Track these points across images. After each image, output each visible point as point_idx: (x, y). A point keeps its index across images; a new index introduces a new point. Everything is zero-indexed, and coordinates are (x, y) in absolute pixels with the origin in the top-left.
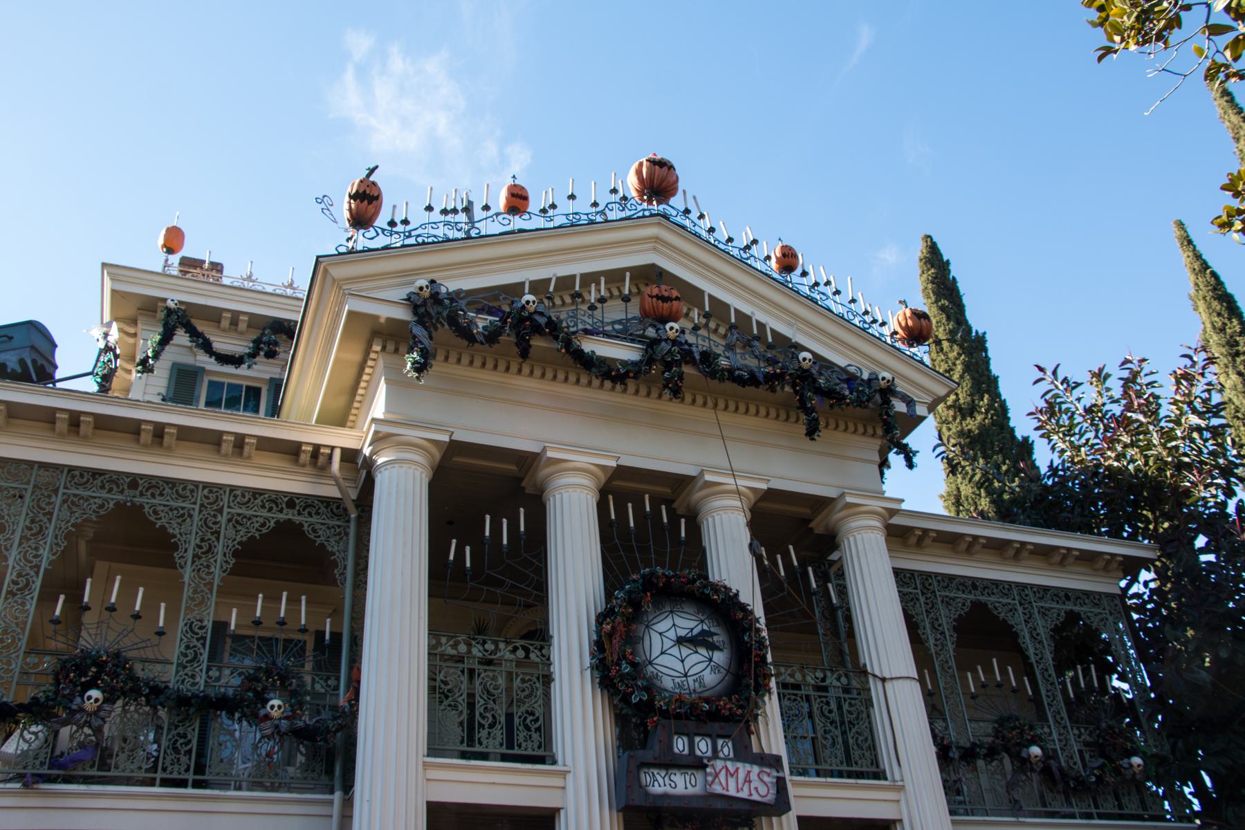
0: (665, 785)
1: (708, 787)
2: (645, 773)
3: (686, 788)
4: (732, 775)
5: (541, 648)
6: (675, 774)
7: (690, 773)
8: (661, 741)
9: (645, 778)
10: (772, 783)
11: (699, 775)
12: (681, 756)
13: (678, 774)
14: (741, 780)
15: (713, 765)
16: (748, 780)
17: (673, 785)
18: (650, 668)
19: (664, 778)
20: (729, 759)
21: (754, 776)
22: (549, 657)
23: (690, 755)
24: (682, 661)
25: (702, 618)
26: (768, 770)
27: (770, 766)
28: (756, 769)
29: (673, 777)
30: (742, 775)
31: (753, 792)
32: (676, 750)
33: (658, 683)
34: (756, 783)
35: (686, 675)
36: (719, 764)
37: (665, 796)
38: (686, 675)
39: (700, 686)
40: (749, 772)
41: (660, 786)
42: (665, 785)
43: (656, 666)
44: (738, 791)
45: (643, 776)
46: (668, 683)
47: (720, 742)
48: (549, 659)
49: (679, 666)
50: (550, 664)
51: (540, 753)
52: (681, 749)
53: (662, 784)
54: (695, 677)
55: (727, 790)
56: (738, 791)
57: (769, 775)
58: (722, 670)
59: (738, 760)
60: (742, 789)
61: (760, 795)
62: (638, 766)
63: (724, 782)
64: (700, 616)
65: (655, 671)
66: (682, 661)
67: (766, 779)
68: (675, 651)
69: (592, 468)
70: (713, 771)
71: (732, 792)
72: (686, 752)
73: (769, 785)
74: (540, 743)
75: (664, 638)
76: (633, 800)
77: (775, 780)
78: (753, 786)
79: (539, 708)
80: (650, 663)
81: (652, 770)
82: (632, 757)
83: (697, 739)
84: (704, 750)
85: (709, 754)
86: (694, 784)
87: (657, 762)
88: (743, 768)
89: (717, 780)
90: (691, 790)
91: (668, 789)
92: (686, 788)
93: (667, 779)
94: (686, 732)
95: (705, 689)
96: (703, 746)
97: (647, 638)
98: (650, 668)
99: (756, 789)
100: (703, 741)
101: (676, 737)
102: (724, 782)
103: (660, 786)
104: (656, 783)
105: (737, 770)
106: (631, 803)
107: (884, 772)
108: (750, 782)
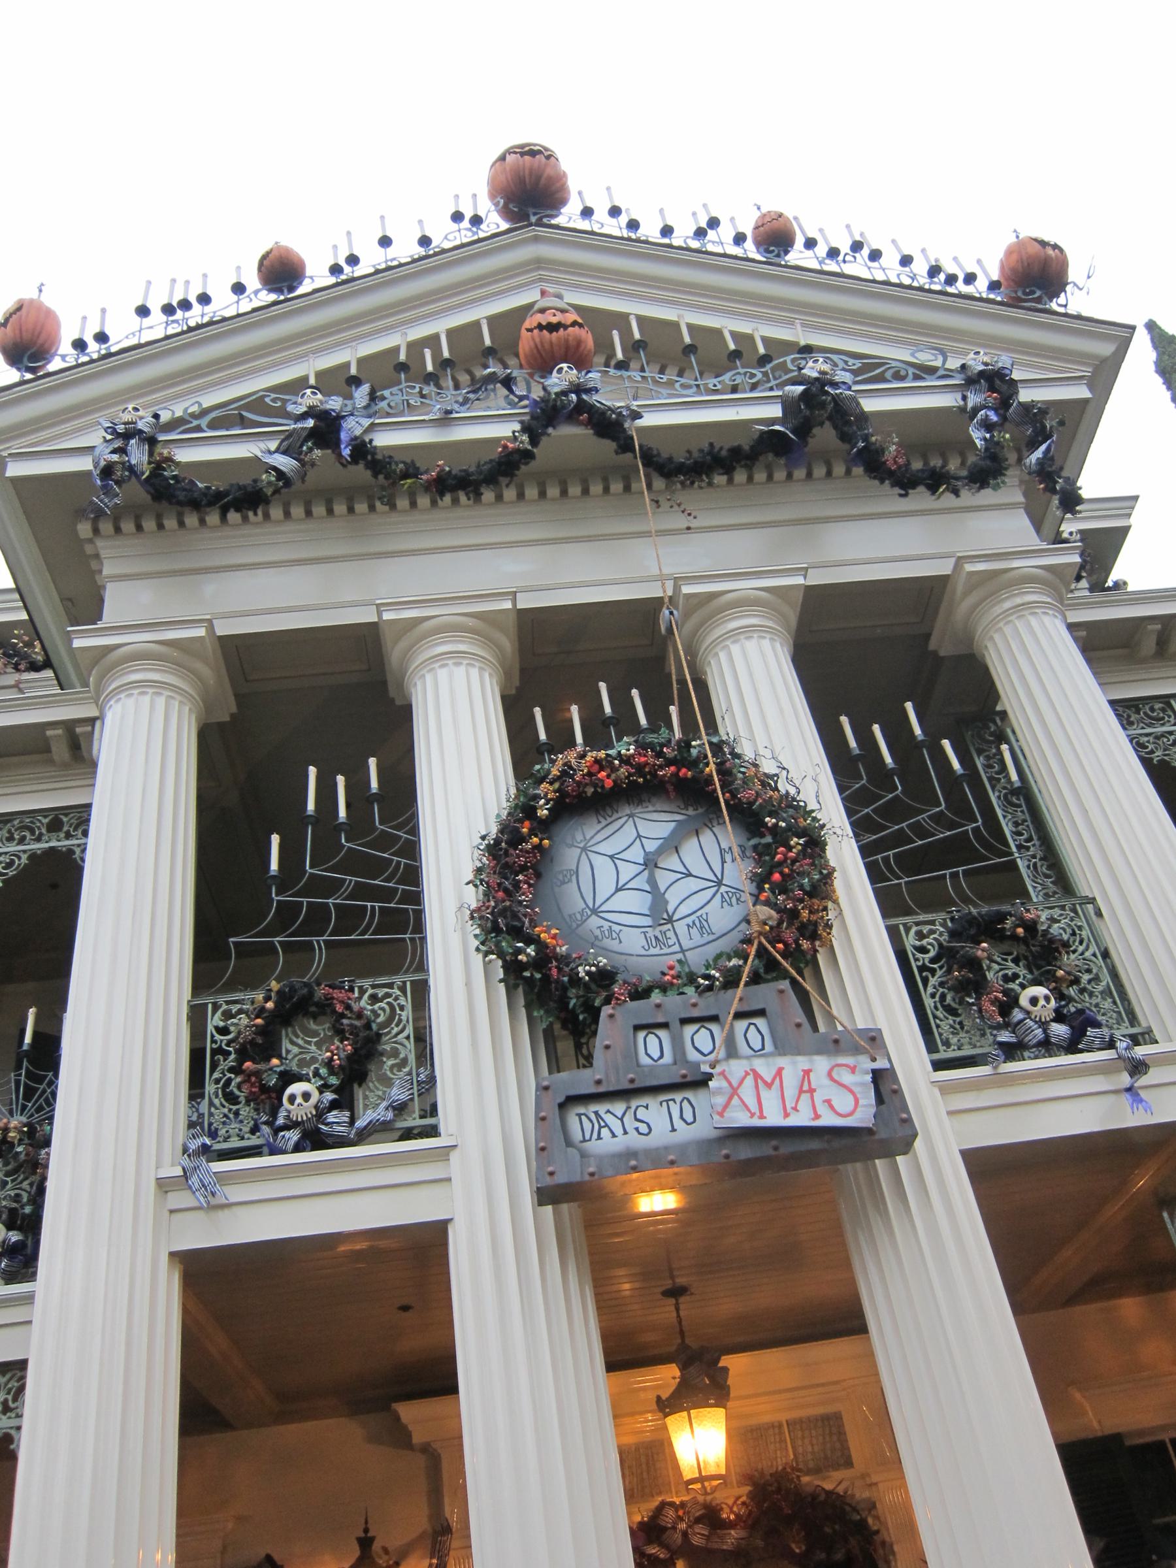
0: (625, 1133)
1: (716, 1117)
2: (579, 1115)
4: (769, 1085)
6: (647, 1107)
7: (678, 1099)
8: (607, 1047)
9: (578, 1122)
10: (862, 1084)
11: (697, 1097)
14: (790, 1092)
15: (723, 1073)
16: (806, 1088)
17: (643, 1128)
19: (621, 1119)
21: (819, 1078)
23: (675, 1063)
26: (849, 1060)
27: (857, 1050)
28: (821, 1064)
29: (641, 1113)
30: (791, 1080)
31: (822, 1109)
32: (645, 1060)
34: (824, 1089)
36: (736, 1068)
39: (702, 935)
40: (807, 1073)
41: (614, 1136)
42: (625, 1133)
43: (601, 914)
44: (786, 1115)
52: (656, 1055)
53: (618, 1131)
54: (689, 920)
55: (762, 1117)
56: (786, 1115)
57: (853, 1070)
60: (795, 1109)
62: (562, 1106)
63: (752, 1102)
67: (847, 1078)
69: (470, 622)
70: (725, 1084)
71: (774, 1118)
72: (668, 1058)
73: (856, 1090)
75: (616, 861)
76: (551, 1174)
77: (869, 1078)
78: (818, 1097)
79: (406, 1042)
80: (595, 911)
81: (593, 1107)
83: (689, 1029)
84: (706, 1047)
86: (690, 1119)
87: (602, 1089)
88: (792, 1067)
89: (735, 1100)
90: (685, 1133)
92: (674, 1130)
94: (661, 1019)
95: (711, 937)
96: (701, 1039)
97: (585, 869)
99: (828, 1102)
101: (641, 1035)
102: (752, 1102)
104: (605, 1131)
105: (779, 1072)
106: (548, 1181)
107: (1149, 1031)
108: (812, 1091)
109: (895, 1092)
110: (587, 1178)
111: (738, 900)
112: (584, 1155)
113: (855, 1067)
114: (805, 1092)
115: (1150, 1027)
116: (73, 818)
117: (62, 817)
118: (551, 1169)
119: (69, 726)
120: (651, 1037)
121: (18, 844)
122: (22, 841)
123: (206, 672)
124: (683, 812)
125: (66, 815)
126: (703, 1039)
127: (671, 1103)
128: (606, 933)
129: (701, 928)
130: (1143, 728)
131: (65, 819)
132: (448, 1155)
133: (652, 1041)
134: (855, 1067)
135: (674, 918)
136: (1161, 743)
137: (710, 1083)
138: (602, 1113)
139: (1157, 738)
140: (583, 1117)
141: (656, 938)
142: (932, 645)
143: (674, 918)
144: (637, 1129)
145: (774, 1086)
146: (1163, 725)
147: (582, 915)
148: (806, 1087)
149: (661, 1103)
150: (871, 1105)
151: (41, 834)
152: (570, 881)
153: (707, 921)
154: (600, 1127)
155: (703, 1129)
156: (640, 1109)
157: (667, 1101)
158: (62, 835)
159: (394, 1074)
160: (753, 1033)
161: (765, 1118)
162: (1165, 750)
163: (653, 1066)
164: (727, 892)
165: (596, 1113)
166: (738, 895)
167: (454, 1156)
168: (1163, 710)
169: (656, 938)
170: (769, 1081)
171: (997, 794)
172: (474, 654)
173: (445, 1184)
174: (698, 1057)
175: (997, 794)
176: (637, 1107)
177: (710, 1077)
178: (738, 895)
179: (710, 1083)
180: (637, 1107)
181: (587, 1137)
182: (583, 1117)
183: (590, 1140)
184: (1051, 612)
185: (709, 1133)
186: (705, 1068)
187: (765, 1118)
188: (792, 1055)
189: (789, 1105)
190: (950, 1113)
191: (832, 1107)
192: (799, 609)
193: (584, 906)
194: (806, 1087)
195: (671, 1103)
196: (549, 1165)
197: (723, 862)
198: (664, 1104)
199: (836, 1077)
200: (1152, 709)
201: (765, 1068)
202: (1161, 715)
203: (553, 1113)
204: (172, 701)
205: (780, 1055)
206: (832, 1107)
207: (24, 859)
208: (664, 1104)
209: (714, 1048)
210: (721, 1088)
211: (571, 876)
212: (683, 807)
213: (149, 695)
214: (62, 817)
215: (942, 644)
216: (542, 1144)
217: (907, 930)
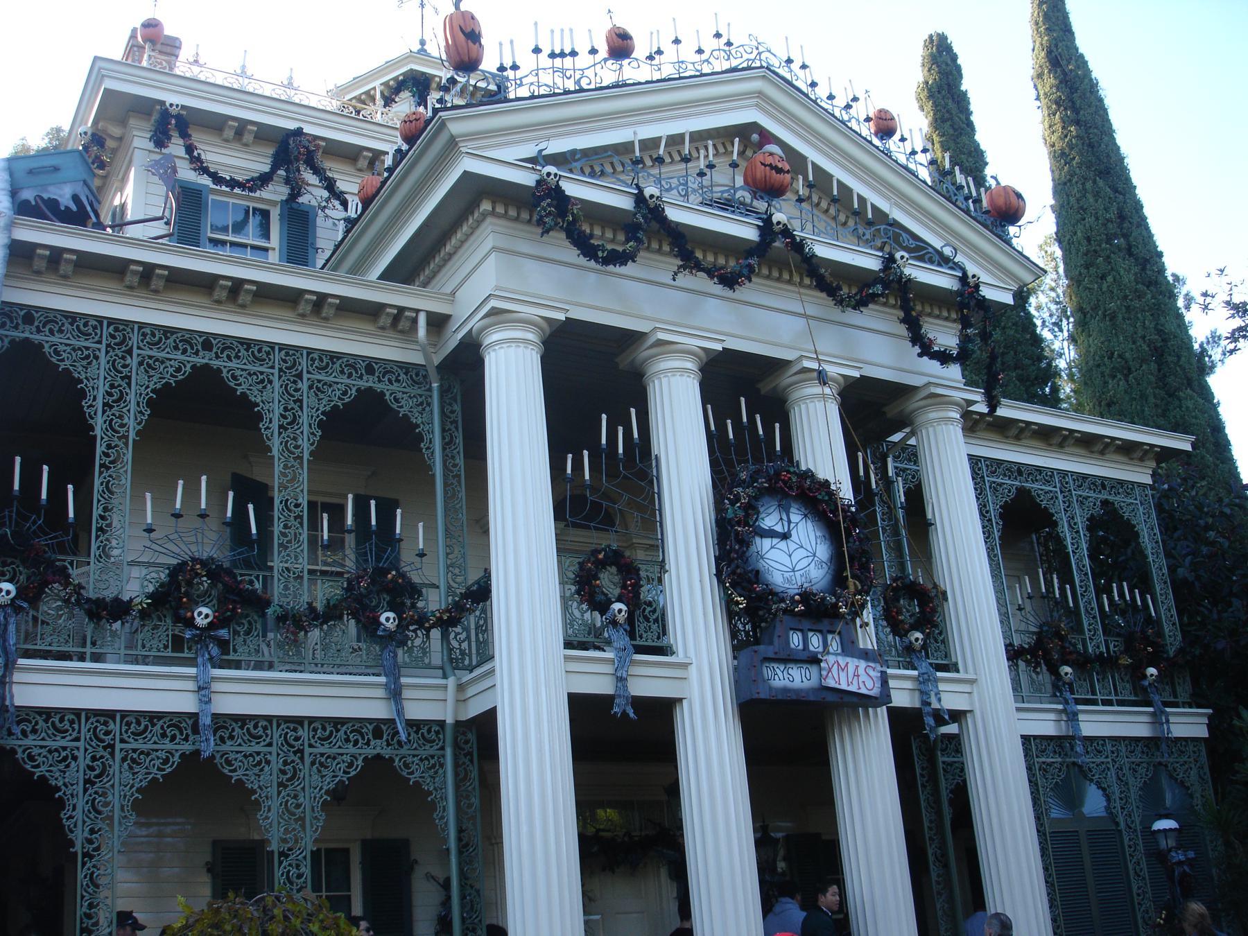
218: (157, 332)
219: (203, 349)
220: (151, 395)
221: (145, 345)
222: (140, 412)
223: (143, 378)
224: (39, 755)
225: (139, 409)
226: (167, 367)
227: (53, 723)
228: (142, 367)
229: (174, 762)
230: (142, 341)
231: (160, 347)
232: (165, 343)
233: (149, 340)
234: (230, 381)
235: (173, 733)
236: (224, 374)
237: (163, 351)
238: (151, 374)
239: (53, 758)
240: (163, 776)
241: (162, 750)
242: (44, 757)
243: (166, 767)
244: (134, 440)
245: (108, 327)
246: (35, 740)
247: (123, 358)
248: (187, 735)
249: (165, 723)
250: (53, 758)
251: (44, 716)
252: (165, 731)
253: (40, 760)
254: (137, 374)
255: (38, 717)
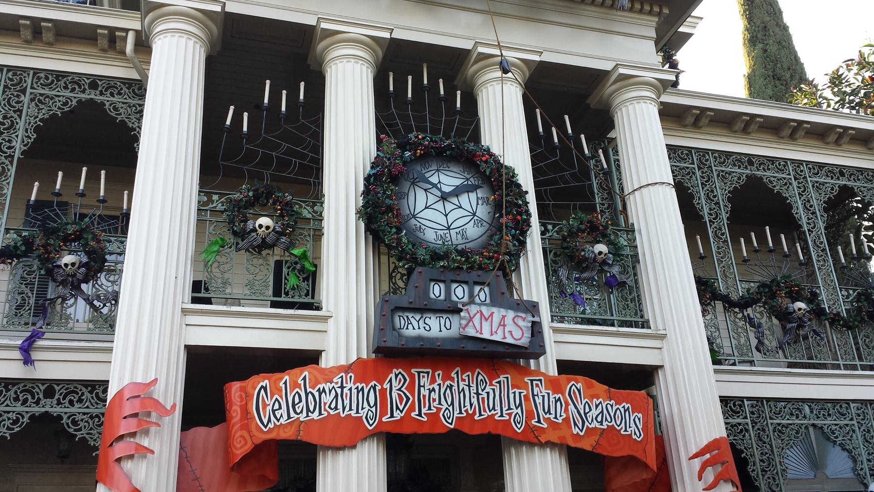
0: (419, 328)
1: (461, 330)
2: (400, 316)
3: (441, 331)
4: (486, 320)
5: (314, 204)
7: (445, 318)
9: (399, 321)
10: (527, 327)
11: (455, 319)
12: (436, 301)
13: (433, 318)
15: (467, 310)
16: (502, 324)
18: (413, 221)
19: (418, 322)
20: (485, 305)
21: (508, 321)
22: (321, 213)
23: (445, 300)
24: (446, 215)
25: (468, 176)
26: (523, 315)
28: (511, 314)
29: (427, 320)
30: (496, 319)
31: (507, 335)
32: (432, 296)
33: (421, 235)
34: (510, 326)
35: (449, 228)
36: (473, 309)
37: (420, 338)
38: (449, 228)
39: (463, 239)
40: (504, 317)
41: (414, 329)
42: (419, 328)
44: (492, 335)
45: (397, 319)
46: (430, 236)
47: (477, 288)
48: (321, 215)
49: (442, 220)
50: (321, 220)
51: (308, 300)
52: (437, 295)
53: (416, 327)
54: (457, 230)
55: (481, 333)
56: (492, 335)
57: (524, 319)
58: (485, 224)
59: (494, 306)
60: (496, 332)
61: (515, 339)
64: (466, 175)
65: (419, 224)
66: (446, 215)
67: (521, 323)
68: (439, 206)
70: (467, 315)
71: (486, 335)
72: (442, 297)
73: (524, 329)
74: (308, 291)
76: (385, 341)
77: (530, 324)
78: (507, 329)
80: (414, 216)
82: (387, 301)
83: (454, 285)
84: (460, 295)
85: (466, 299)
86: (448, 328)
87: (411, 306)
88: (498, 313)
89: (471, 324)
90: (445, 333)
91: (422, 332)
92: (441, 331)
93: (421, 322)
94: (443, 278)
96: (460, 292)
98: (413, 221)
99: (510, 332)
100: (460, 286)
101: (432, 284)
103: (414, 329)
104: (410, 326)
105: (493, 313)
106: (383, 344)
107: (648, 321)
108: (504, 326)
109: (540, 332)
110: (400, 346)
111: (481, 224)
112: (400, 335)
113: (525, 318)
114: (502, 325)
115: (649, 320)
116: (105, 83)
117: (98, 81)
118: (385, 339)
119: (112, 30)
120: (436, 286)
121: (71, 92)
122: (73, 90)
123: (215, 29)
124: (462, 174)
125: (101, 80)
126: (459, 291)
127: (441, 318)
128: (418, 228)
129: (463, 235)
130: (675, 162)
131: (100, 83)
132: (327, 320)
133: (437, 287)
134: (525, 318)
135: (451, 228)
136: (682, 172)
137: (461, 313)
138: (410, 317)
139: (680, 169)
140: (401, 317)
141: (441, 236)
142: (588, 101)
143: (451, 228)
144: (424, 328)
145: (488, 321)
146: (685, 162)
147: (408, 217)
148: (502, 324)
149: (437, 317)
150: (529, 337)
151: (85, 89)
152: (404, 198)
153: (465, 232)
154: (408, 324)
155: (454, 332)
156: (427, 318)
157: (440, 317)
158: (98, 92)
159: (301, 275)
160: (483, 294)
161: (483, 334)
162: (682, 176)
163: (435, 299)
164: (477, 220)
165: (407, 317)
166: (482, 223)
167: (331, 321)
168: (687, 155)
169: (441, 236)
170: (487, 318)
171: (597, 181)
172: (368, 60)
173: (324, 333)
174: (456, 299)
175: (597, 181)
176: (426, 317)
177: (461, 310)
178: (482, 223)
179: (461, 313)
180: (426, 317)
181: (402, 328)
182: (401, 317)
183: (403, 329)
184: (653, 103)
185: (457, 335)
186: (460, 306)
187: (483, 334)
188: (499, 307)
189: (493, 331)
190: (555, 342)
191: (512, 334)
192: (532, 72)
193: (409, 213)
194: (502, 324)
195: (441, 318)
196: (384, 338)
197: (478, 204)
198: (438, 318)
199: (516, 321)
200: (682, 153)
201: (486, 311)
202: (686, 157)
203: (389, 314)
204: (197, 45)
205: (493, 306)
206: (512, 334)
207: (74, 103)
208: (438, 318)
209: (464, 296)
210: (465, 317)
211: (405, 196)
212: (462, 171)
213: (185, 38)
214: (98, 81)
215: (593, 102)
216: (381, 327)
217: (550, 252)
218: (50, 76)
219: (90, 88)
220: (39, 123)
221: (38, 86)
222: (28, 137)
223: (33, 110)
224: (82, 420)
225: (27, 135)
226: (56, 102)
227: (97, 394)
228: (34, 103)
229: (23, 423)
230: (37, 83)
231: (52, 87)
232: (56, 84)
233: (42, 82)
234: (111, 112)
235: (25, 397)
236: (107, 106)
237: (54, 89)
238: (41, 107)
239: (94, 423)
240: (11, 435)
241: (14, 412)
242: (86, 422)
243: (15, 427)
244: (19, 158)
245: (7, 73)
246: (80, 408)
247: (18, 96)
248: (39, 399)
249: (19, 389)
250: (94, 423)
251: (90, 388)
252: (19, 396)
253: (82, 424)
254: (29, 108)
255: (84, 390)
